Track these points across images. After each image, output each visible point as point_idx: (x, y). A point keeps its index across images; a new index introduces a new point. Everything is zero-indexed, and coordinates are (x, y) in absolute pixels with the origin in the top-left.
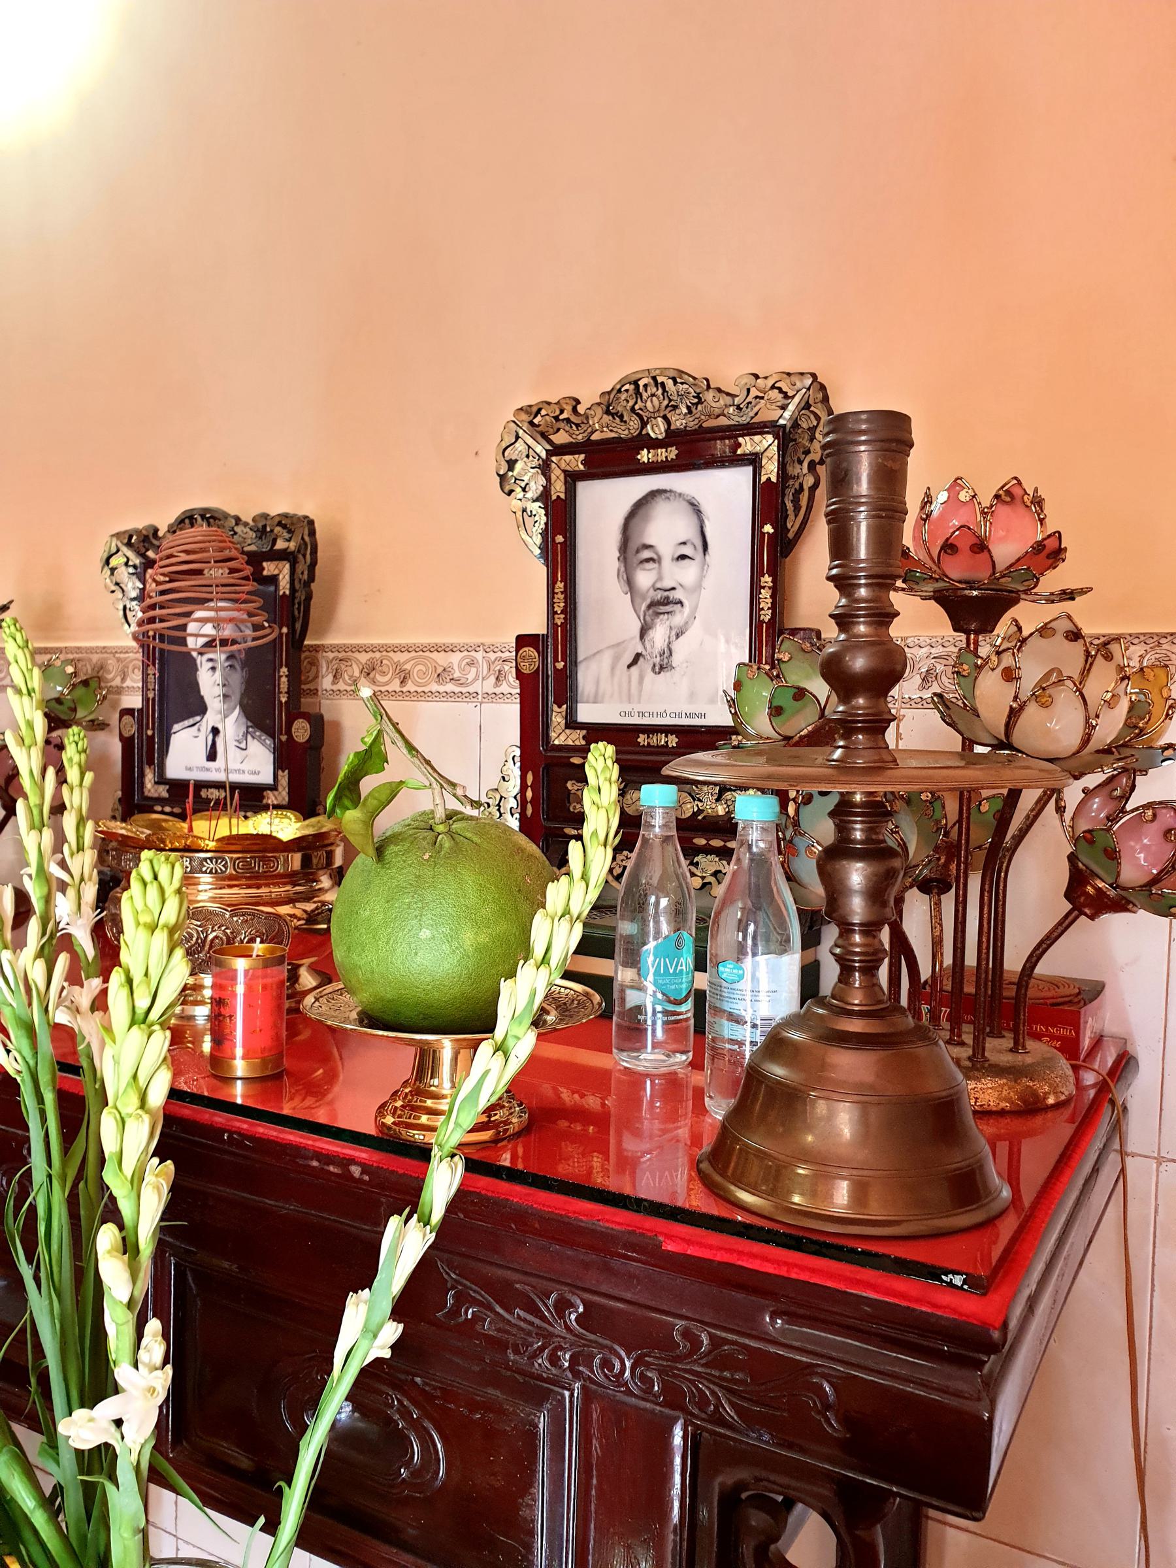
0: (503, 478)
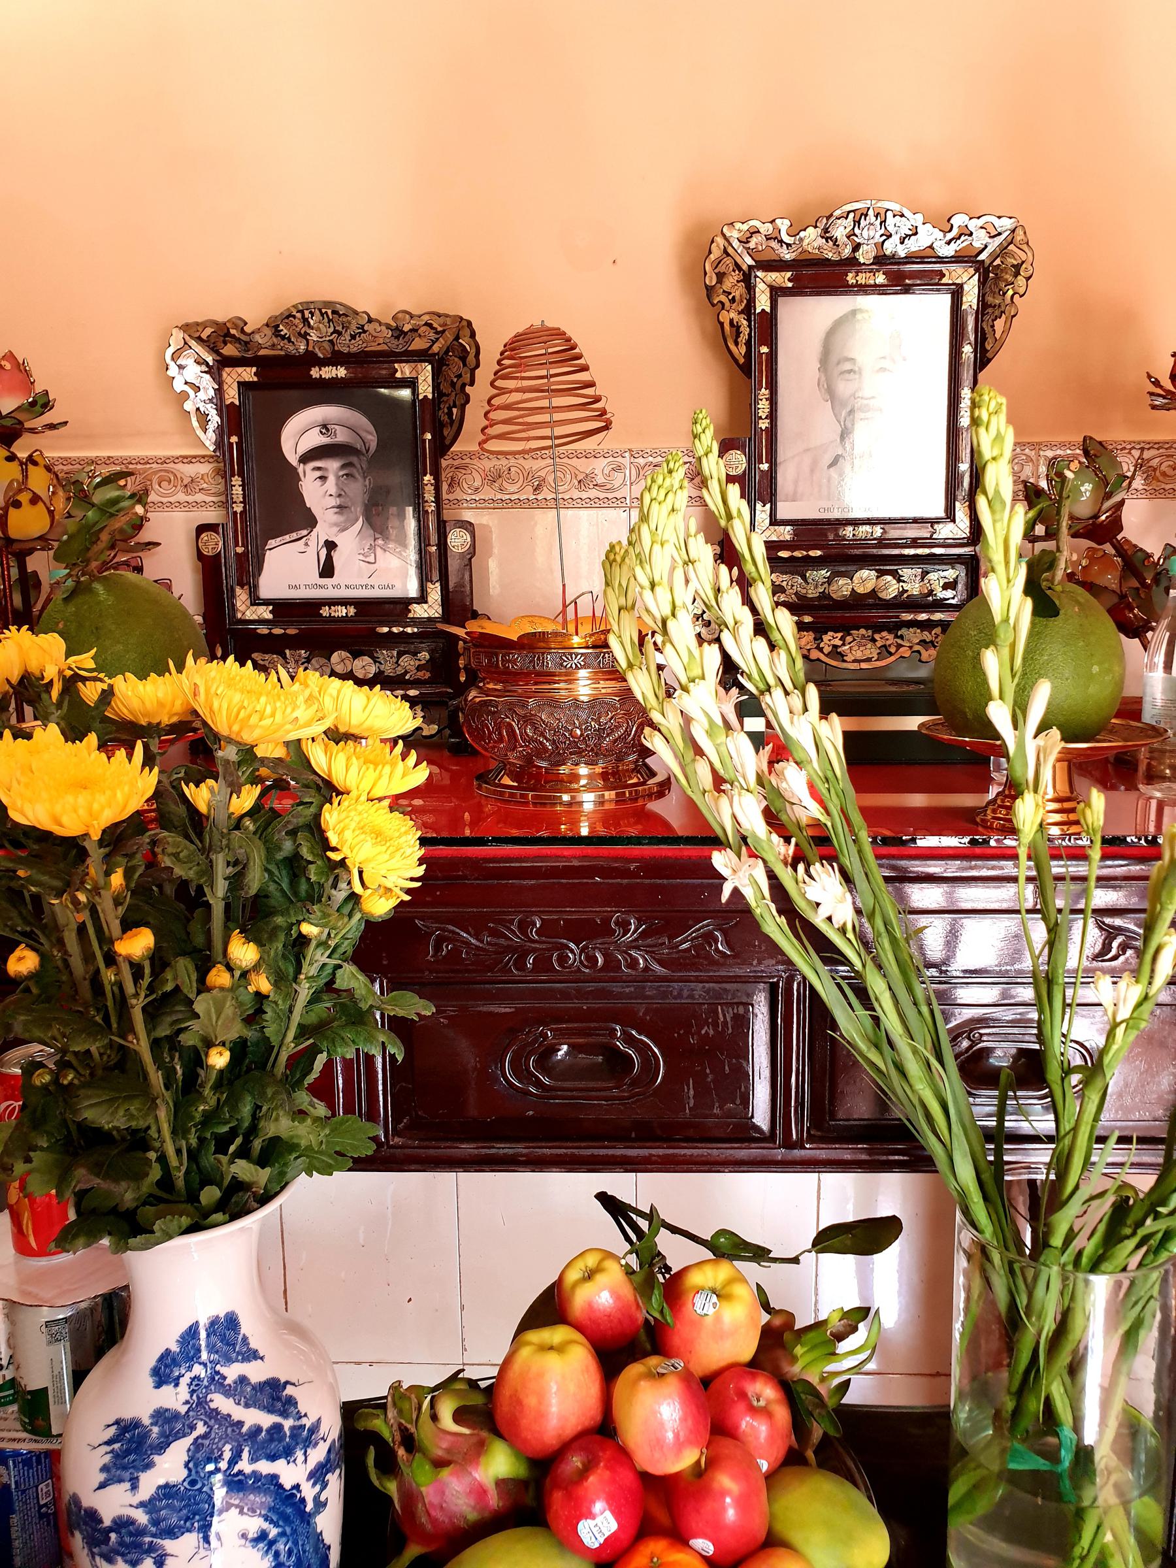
0: (710, 290)
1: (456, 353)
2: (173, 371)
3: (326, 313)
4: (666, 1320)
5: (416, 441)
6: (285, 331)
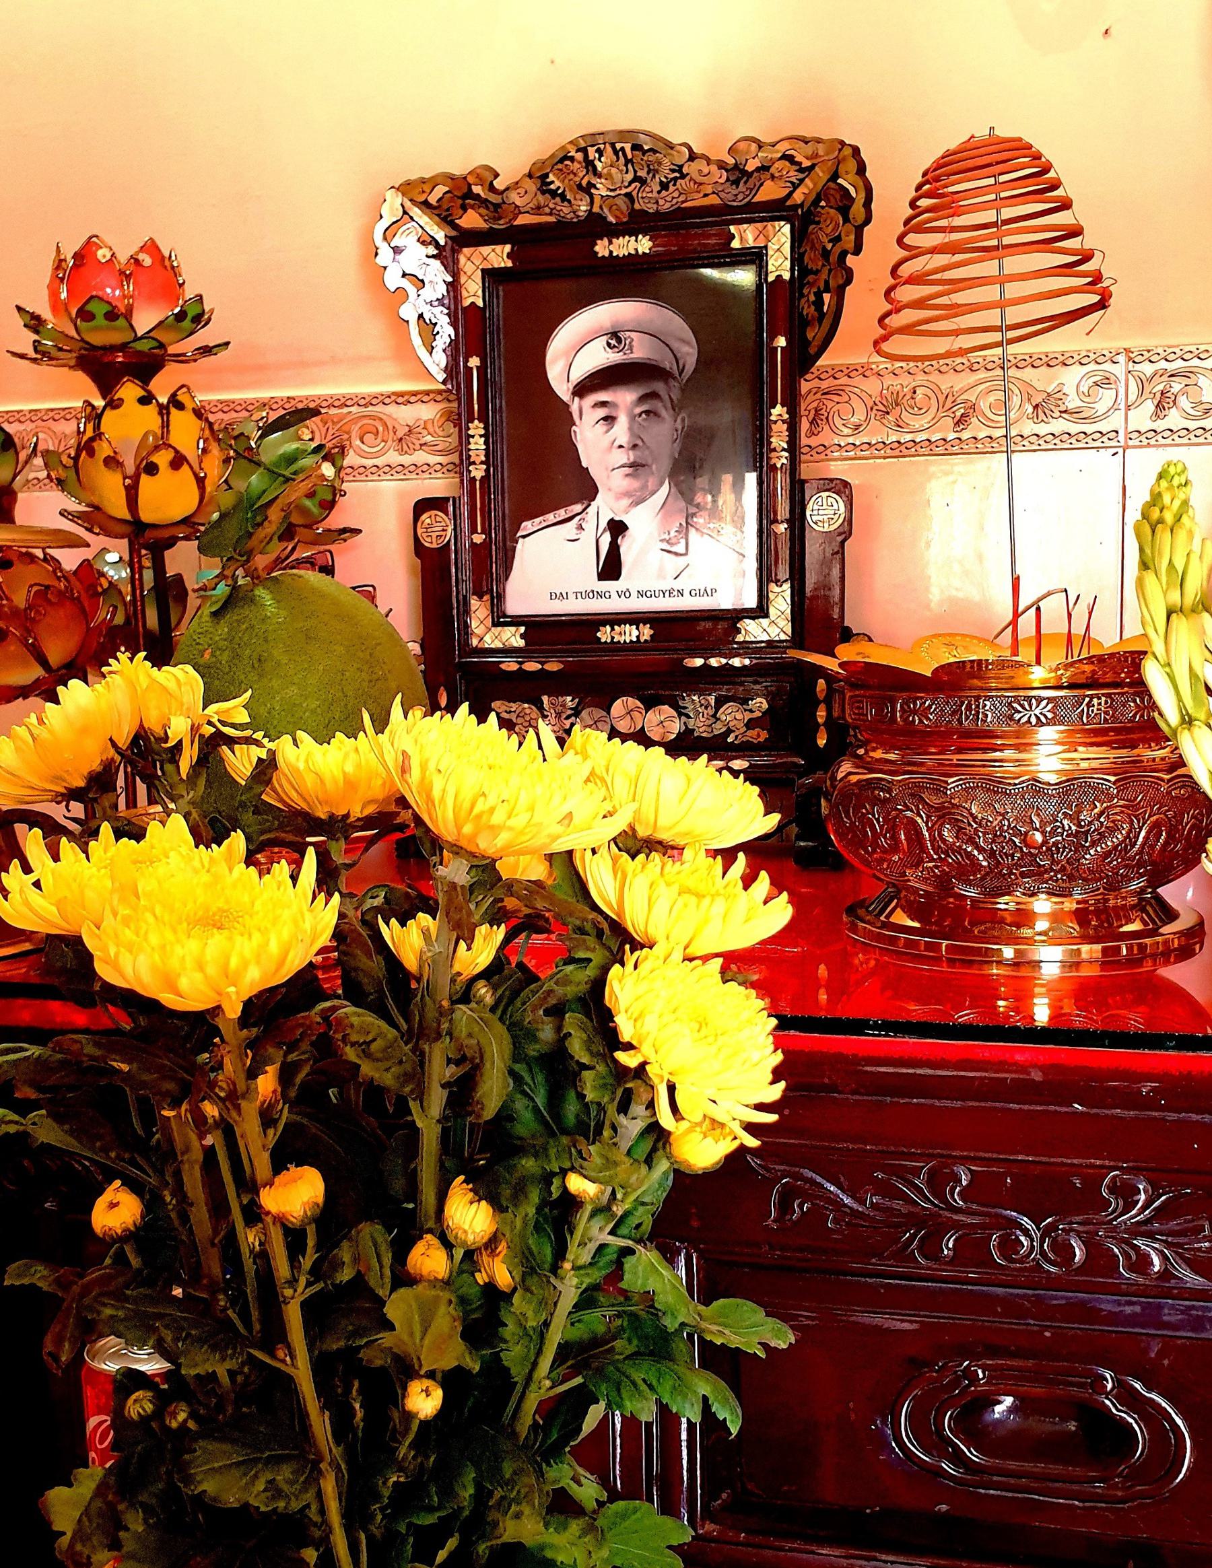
1: (833, 203)
2: (385, 255)
3: (622, 149)
5: (759, 352)
6: (556, 182)
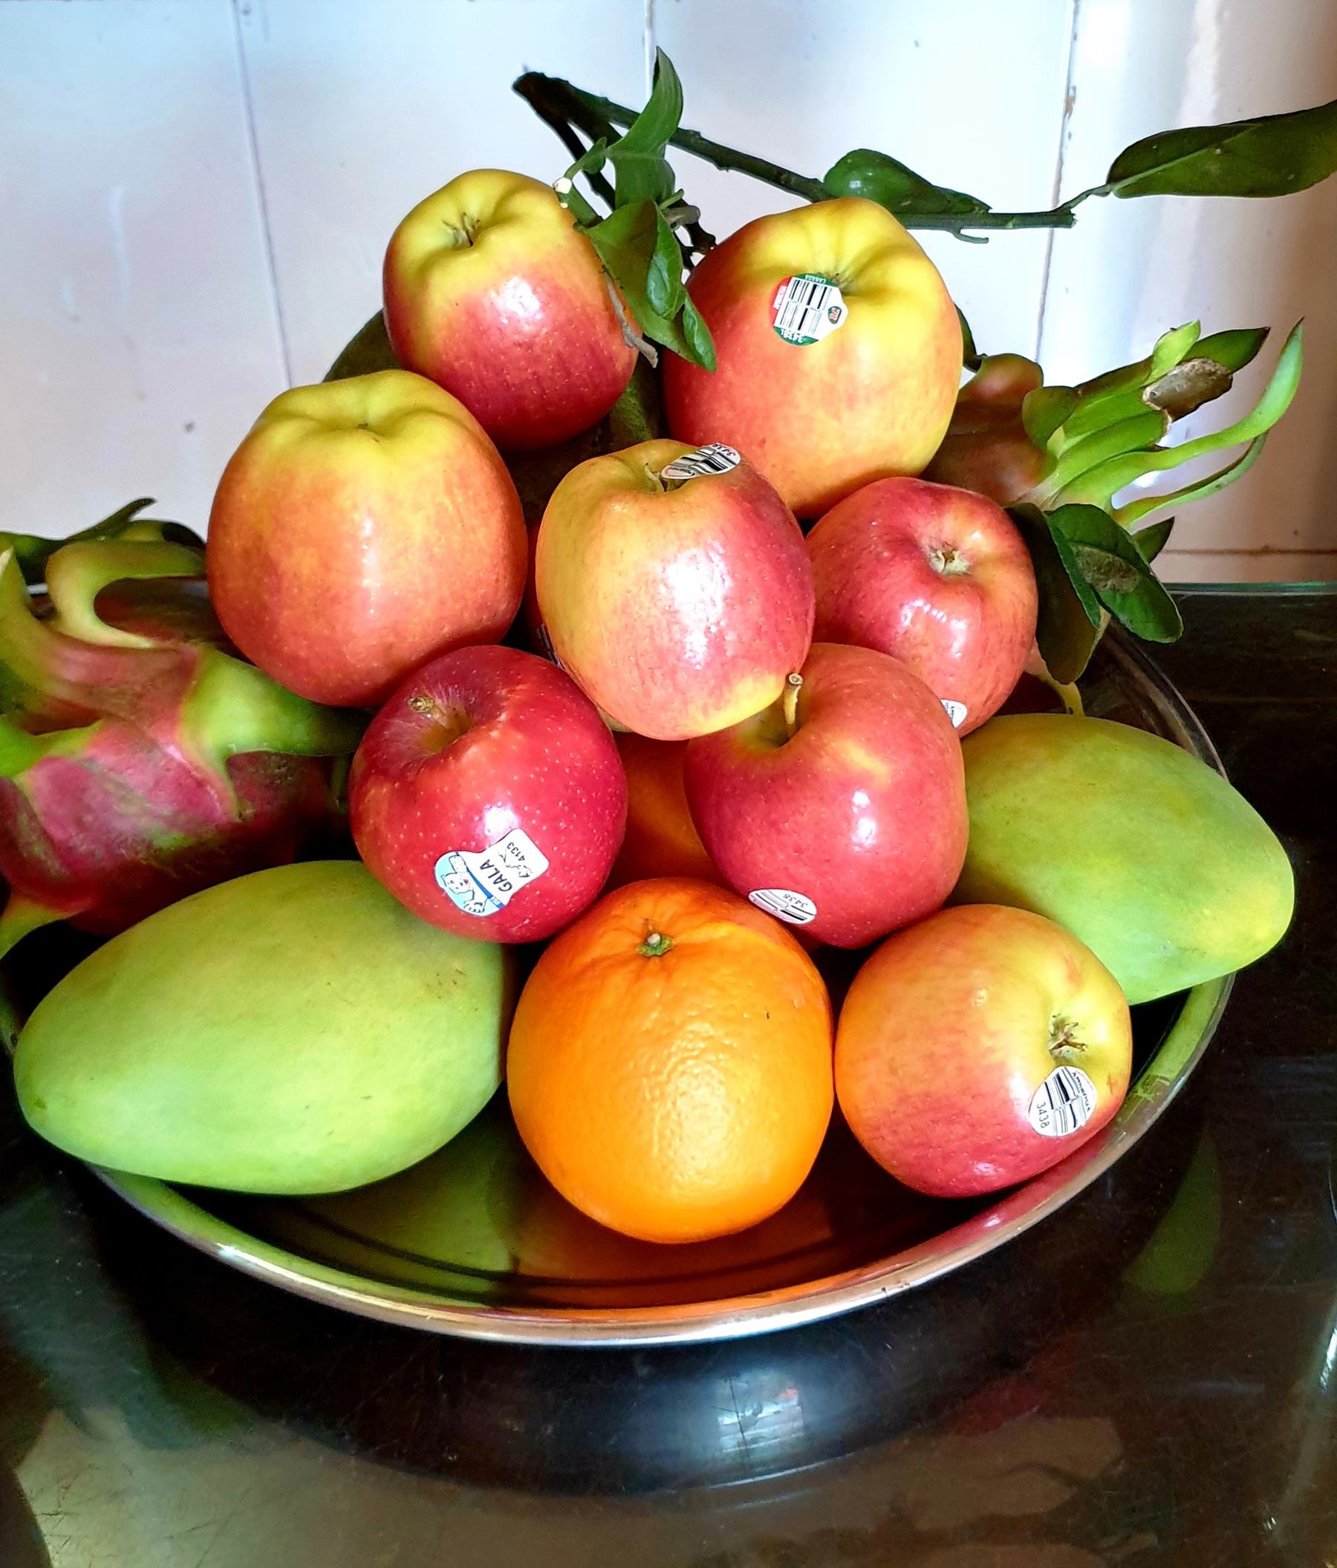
4: (690, 348)
